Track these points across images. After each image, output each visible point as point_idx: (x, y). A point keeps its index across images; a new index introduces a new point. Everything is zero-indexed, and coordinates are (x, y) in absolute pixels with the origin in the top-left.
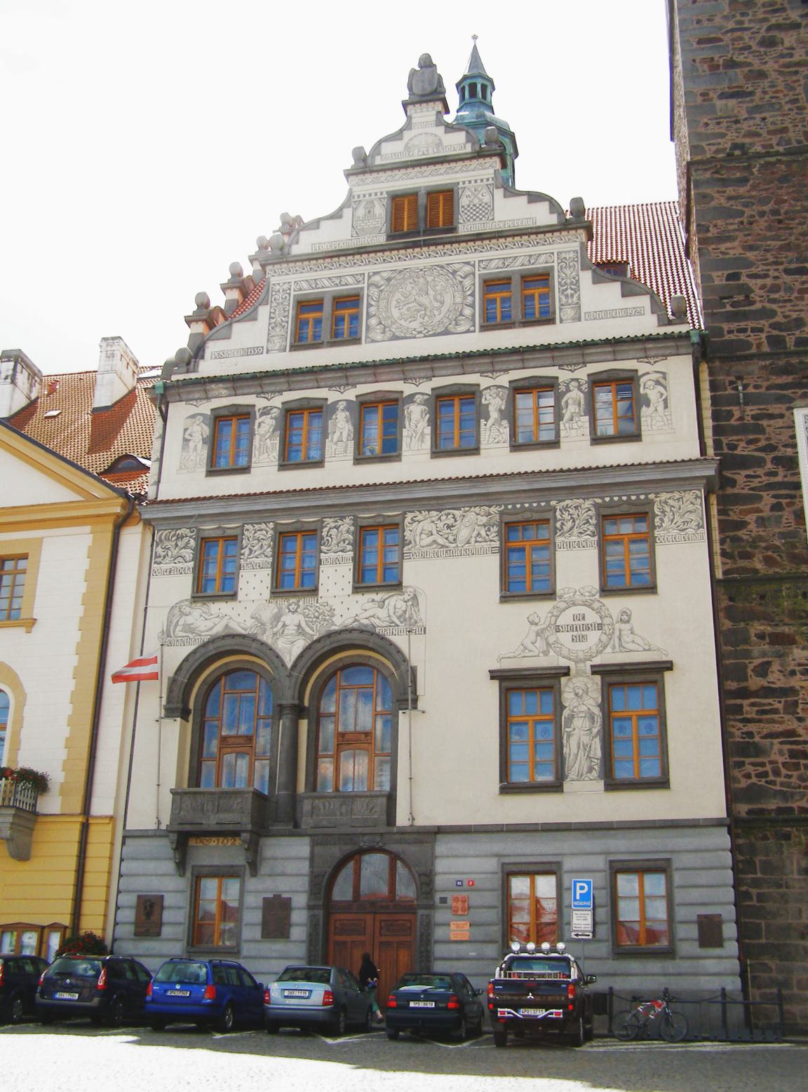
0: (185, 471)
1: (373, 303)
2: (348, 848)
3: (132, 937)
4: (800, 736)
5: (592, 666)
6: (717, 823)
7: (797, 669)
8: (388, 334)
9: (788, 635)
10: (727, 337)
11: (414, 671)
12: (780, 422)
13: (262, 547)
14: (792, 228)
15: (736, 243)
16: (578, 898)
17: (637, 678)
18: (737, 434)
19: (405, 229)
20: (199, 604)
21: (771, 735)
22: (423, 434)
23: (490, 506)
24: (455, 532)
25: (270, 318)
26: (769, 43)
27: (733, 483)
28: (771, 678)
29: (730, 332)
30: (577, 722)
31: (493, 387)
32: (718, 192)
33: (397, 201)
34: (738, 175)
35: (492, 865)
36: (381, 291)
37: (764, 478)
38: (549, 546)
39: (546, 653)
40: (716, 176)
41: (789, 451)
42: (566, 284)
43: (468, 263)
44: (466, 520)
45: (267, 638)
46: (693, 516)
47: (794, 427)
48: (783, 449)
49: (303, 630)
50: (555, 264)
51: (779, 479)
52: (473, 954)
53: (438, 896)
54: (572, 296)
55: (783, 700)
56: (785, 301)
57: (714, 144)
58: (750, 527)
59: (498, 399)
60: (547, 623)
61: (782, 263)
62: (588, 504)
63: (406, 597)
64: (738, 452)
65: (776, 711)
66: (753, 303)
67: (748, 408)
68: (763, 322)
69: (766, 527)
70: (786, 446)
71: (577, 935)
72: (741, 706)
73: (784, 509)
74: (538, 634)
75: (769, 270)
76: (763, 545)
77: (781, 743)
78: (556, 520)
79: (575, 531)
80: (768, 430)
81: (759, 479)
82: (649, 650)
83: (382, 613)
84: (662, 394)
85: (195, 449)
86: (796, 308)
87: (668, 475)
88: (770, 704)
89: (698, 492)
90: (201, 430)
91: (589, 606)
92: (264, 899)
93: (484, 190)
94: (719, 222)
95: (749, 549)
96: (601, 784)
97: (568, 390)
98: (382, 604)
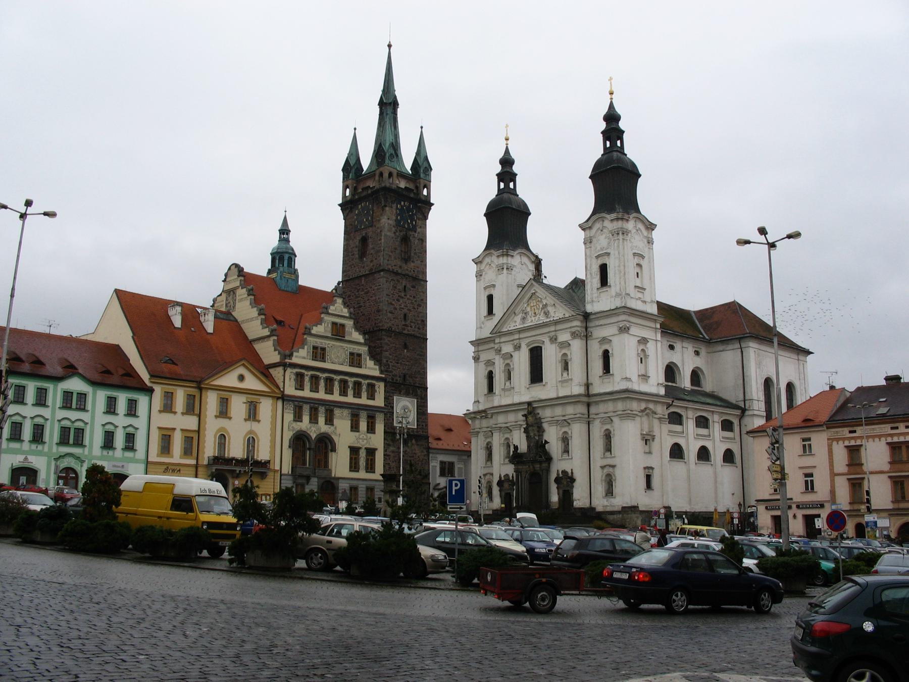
26: (398, 300)
31: (351, 380)
33: (334, 324)
87: (377, 409)
90: (293, 377)
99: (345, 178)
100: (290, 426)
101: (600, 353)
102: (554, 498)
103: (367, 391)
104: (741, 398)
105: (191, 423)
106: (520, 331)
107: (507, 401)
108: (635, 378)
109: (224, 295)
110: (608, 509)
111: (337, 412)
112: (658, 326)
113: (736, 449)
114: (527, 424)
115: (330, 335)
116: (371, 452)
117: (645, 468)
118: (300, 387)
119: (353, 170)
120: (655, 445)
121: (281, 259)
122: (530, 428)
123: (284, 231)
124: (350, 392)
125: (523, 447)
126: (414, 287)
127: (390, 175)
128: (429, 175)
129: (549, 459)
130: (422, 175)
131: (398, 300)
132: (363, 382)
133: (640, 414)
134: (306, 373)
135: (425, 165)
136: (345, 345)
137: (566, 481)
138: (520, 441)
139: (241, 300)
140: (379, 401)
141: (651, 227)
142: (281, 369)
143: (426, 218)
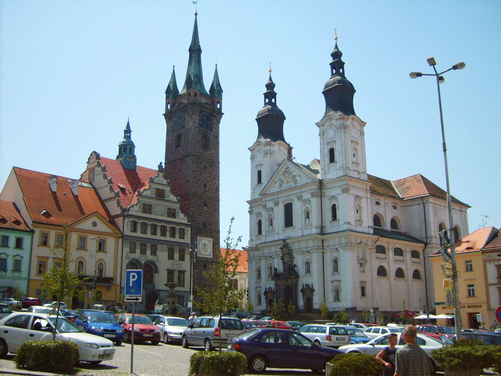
33: (157, 190)
45: (140, 260)
90: (129, 224)
99: (167, 97)
100: (127, 255)
101: (330, 206)
102: (301, 303)
103: (179, 233)
104: (424, 236)
105: (60, 253)
106: (278, 193)
107: (270, 239)
108: (353, 222)
109: (87, 172)
110: (336, 310)
111: (159, 247)
112: (368, 188)
113: (421, 269)
114: (283, 254)
115: (154, 197)
116: (182, 272)
117: (361, 282)
118: (134, 230)
119: (172, 93)
120: (367, 267)
121: (125, 149)
122: (285, 257)
123: (128, 131)
124: (168, 234)
125: (281, 269)
126: (211, 166)
127: (195, 95)
128: (221, 95)
129: (297, 276)
130: (216, 95)
131: (201, 175)
132: (177, 227)
133: (357, 246)
134: (138, 221)
135: (219, 88)
137: (309, 291)
138: (278, 265)
139: (98, 175)
140: (188, 239)
141: (363, 124)
142: (121, 219)
143: (219, 122)
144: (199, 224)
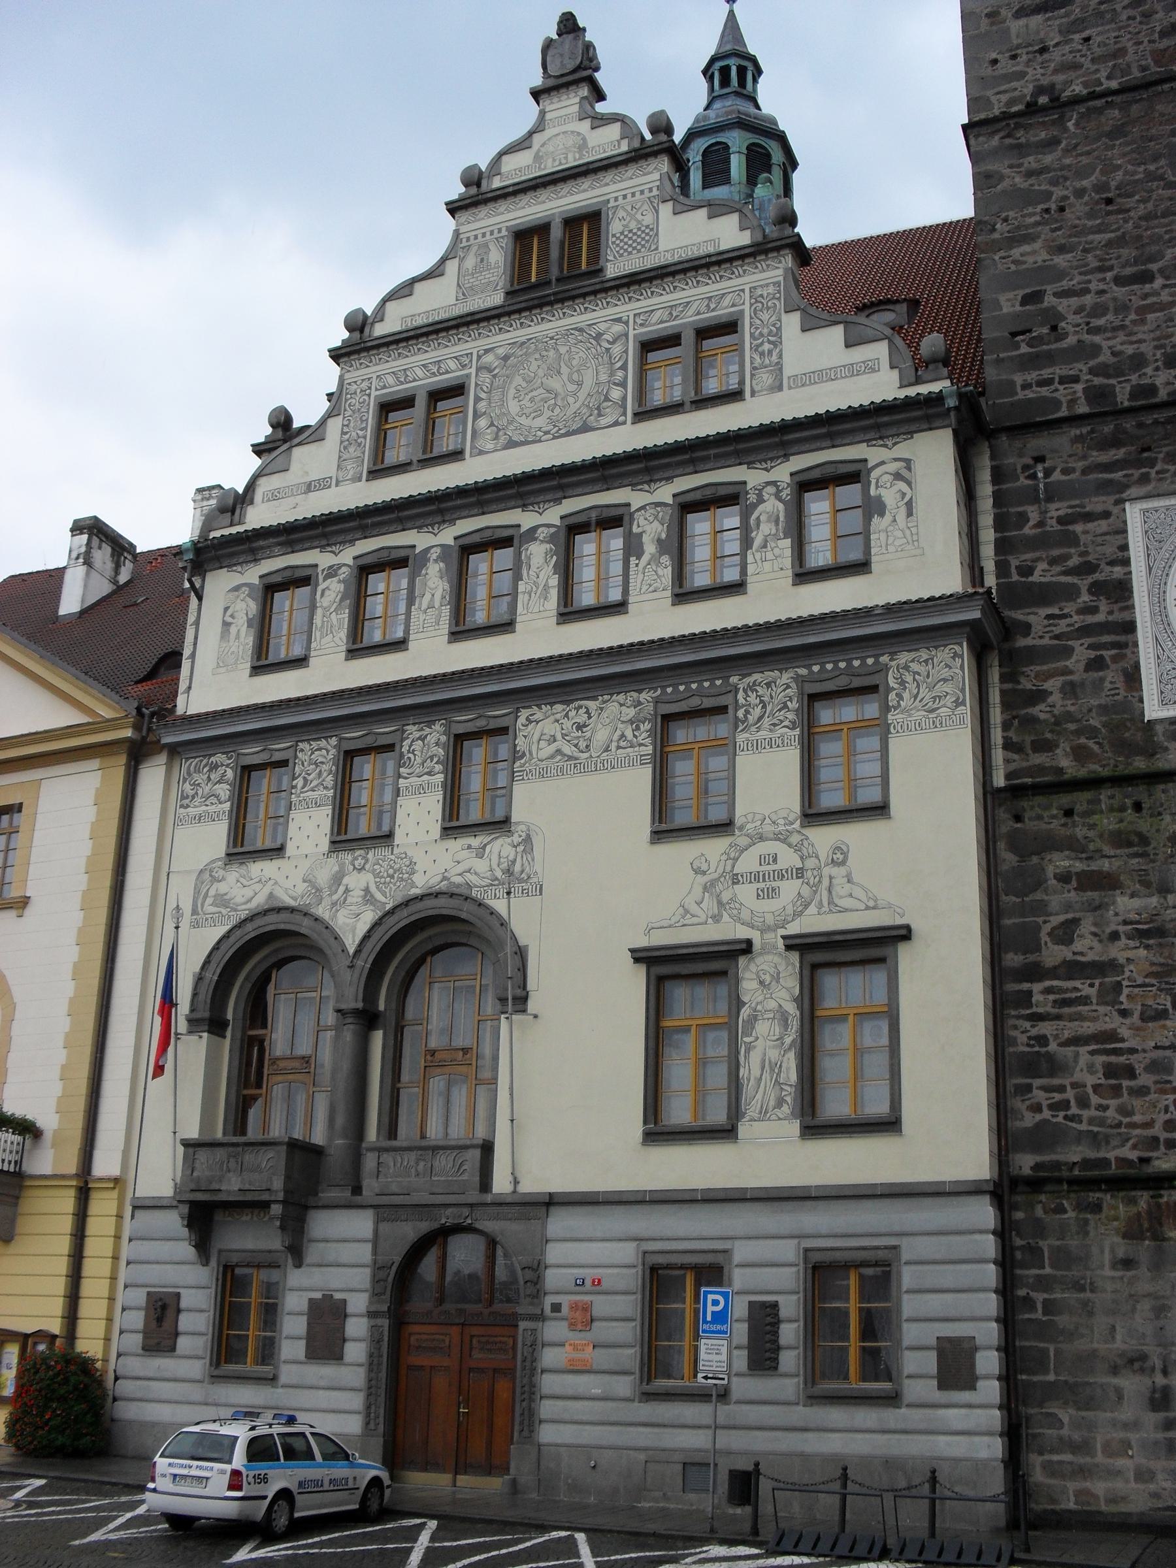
0: (223, 670)
1: (483, 395)
2: (425, 1227)
3: (140, 1351)
4: (1123, 1040)
5: (784, 937)
6: (972, 1190)
7: (1121, 928)
8: (503, 440)
9: (1108, 873)
10: (1021, 395)
11: (521, 953)
12: (1103, 525)
13: (320, 773)
14: (1128, 210)
15: (1037, 245)
16: (709, 1318)
17: (700, 967)
18: (1034, 549)
19: (533, 280)
20: (235, 867)
21: (1076, 1041)
22: (546, 587)
23: (640, 691)
24: (588, 734)
25: (343, 433)
27: (1026, 628)
28: (1078, 946)
29: (1026, 386)
30: (762, 1028)
32: (1011, 167)
34: (1043, 135)
35: (628, 1252)
36: (494, 376)
37: (1076, 618)
38: (728, 747)
39: (717, 918)
40: (1008, 141)
41: (1118, 571)
42: (761, 335)
43: (619, 320)
44: (605, 714)
45: (322, 911)
46: (948, 688)
47: (1125, 531)
48: (1109, 568)
49: (372, 896)
50: (747, 307)
51: (1100, 617)
52: (597, 1391)
53: (549, 1301)
54: (770, 352)
55: (1097, 982)
56: (1115, 329)
57: (1005, 92)
58: (1050, 700)
59: (656, 524)
60: (720, 870)
61: (1111, 268)
62: (786, 677)
63: (516, 839)
64: (1036, 578)
65: (1085, 1001)
66: (1066, 335)
67: (1052, 506)
68: (1080, 366)
69: (1077, 698)
70: (1111, 563)
71: (706, 1378)
72: (1030, 993)
73: (1108, 667)
74: (705, 889)
75: (1089, 282)
76: (1072, 727)
77: (1092, 1053)
78: (737, 707)
79: (766, 721)
80: (1083, 538)
81: (1068, 621)
82: (874, 908)
83: (481, 866)
84: (904, 495)
85: (238, 637)
86: (1134, 338)
87: (909, 627)
88: (1076, 989)
89: (956, 647)
90: (246, 607)
91: (784, 841)
92: (310, 1300)
93: (646, 207)
94: (1011, 214)
95: (1048, 736)
96: (795, 1127)
97: (761, 500)
98: (481, 852)
136: (601, 315)
144: (1138, 361)
